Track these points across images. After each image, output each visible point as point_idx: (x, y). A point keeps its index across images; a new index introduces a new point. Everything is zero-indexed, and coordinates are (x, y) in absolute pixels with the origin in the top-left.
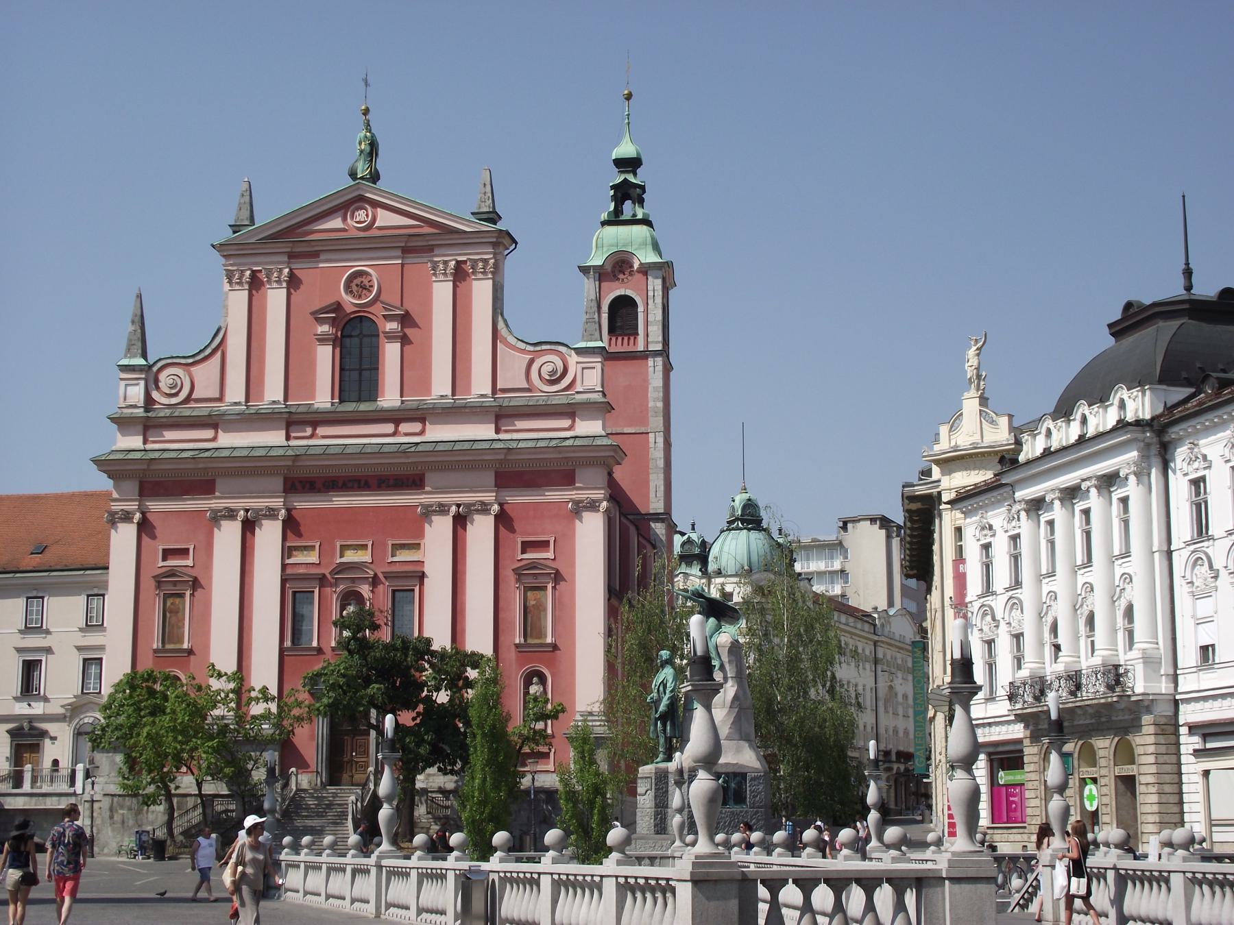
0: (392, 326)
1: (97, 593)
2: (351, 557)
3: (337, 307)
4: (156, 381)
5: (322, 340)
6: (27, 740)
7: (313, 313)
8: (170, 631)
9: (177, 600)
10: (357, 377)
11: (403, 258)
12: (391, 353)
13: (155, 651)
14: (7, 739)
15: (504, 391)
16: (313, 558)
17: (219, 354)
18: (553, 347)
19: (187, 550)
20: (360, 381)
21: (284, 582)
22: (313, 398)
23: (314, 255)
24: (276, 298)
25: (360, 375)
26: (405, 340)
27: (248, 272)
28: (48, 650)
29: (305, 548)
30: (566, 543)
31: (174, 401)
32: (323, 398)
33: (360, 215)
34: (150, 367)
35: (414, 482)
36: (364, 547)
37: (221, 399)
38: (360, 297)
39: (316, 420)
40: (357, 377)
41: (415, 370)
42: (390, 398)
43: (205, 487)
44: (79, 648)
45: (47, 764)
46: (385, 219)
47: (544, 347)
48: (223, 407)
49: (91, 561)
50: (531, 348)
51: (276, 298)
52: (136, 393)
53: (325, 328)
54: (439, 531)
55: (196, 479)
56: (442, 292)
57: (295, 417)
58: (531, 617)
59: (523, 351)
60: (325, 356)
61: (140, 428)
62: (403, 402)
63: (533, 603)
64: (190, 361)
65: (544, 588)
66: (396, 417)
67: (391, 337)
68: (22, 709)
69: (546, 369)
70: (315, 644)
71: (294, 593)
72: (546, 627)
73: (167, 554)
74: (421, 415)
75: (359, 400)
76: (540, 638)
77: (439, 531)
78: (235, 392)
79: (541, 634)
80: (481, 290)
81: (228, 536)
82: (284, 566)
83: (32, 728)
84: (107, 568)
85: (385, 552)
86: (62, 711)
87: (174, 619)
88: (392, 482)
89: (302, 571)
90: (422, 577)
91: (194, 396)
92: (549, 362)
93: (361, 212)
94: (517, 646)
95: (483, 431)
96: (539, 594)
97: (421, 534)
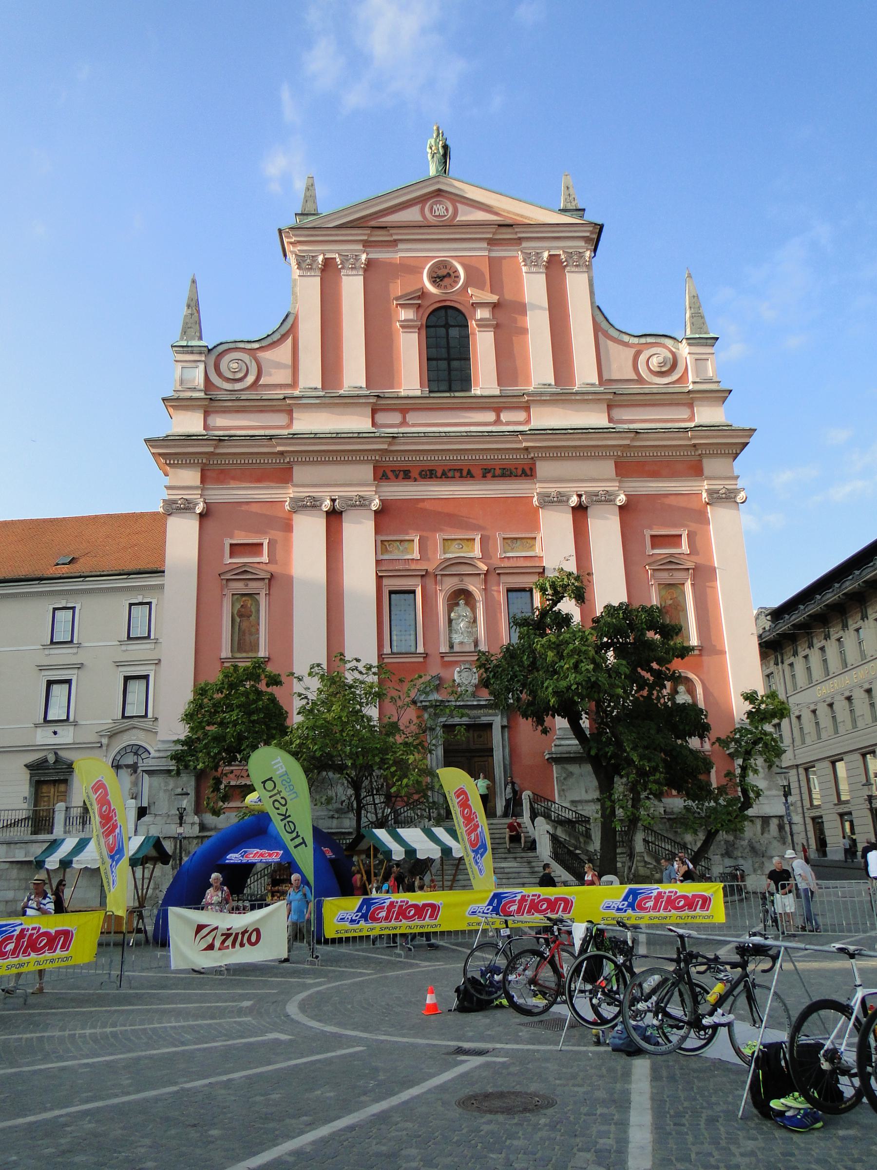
3: (423, 294)
5: (406, 326)
6: (50, 776)
8: (243, 639)
10: (448, 364)
11: (490, 251)
14: (25, 775)
17: (289, 341)
19: (262, 544)
21: (379, 578)
24: (352, 287)
31: (238, 386)
33: (439, 209)
34: (210, 351)
35: (527, 473)
37: (294, 384)
40: (448, 364)
44: (119, 664)
47: (649, 340)
48: (297, 393)
50: (636, 341)
52: (197, 376)
59: (626, 344)
63: (670, 602)
64: (256, 346)
66: (496, 404)
67: (483, 324)
68: (44, 737)
69: (654, 362)
70: (421, 649)
71: (391, 592)
73: (235, 549)
78: (311, 377)
80: (576, 285)
82: (378, 562)
87: (245, 624)
88: (498, 472)
92: (657, 357)
97: (536, 527)
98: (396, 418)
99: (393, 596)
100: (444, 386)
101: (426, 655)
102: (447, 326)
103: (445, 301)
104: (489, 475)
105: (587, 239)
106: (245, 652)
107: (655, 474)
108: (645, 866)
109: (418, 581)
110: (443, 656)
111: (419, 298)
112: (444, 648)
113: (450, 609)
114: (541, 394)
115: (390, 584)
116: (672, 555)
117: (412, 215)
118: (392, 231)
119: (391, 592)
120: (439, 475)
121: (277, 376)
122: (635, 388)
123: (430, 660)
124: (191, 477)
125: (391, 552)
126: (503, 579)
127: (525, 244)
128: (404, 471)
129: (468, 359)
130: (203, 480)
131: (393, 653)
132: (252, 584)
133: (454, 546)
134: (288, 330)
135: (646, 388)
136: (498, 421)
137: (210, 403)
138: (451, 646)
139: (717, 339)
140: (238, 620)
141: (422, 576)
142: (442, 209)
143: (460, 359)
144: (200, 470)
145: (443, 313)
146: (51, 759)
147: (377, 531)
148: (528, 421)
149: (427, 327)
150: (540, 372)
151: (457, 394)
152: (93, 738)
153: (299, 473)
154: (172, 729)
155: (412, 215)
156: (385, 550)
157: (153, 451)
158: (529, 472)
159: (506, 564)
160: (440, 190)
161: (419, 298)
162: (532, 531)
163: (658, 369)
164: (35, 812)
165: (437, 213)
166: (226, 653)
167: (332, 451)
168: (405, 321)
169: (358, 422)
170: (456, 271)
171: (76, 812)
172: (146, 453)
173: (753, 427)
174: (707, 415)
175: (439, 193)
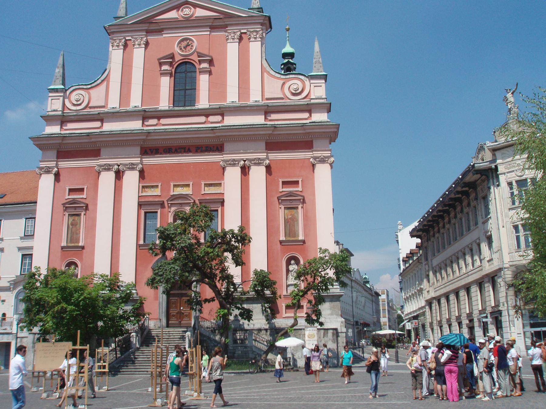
0: (205, 65)
1: (31, 217)
2: (179, 191)
4: (69, 98)
5: (163, 74)
7: (159, 59)
9: (76, 218)
10: (184, 92)
12: (203, 81)
13: (63, 248)
15: (267, 99)
16: (157, 192)
18: (296, 76)
19: (83, 189)
20: (185, 95)
22: (158, 104)
23: (160, 31)
24: (139, 54)
25: (185, 92)
26: (210, 73)
29: (153, 187)
30: (310, 182)
31: (79, 108)
32: (164, 103)
35: (218, 148)
36: (188, 185)
38: (186, 52)
39: (160, 115)
40: (184, 92)
41: (218, 87)
42: (203, 102)
43: (95, 153)
46: (200, 13)
49: (29, 200)
51: (139, 54)
53: (165, 67)
54: (233, 175)
55: (89, 148)
57: (148, 114)
58: (290, 224)
60: (166, 83)
61: (59, 122)
62: (210, 105)
63: (290, 217)
65: (297, 208)
66: (206, 113)
67: (203, 71)
71: (146, 213)
72: (298, 231)
73: (71, 191)
74: (222, 112)
75: (185, 106)
76: (295, 237)
77: (233, 175)
79: (295, 234)
81: (107, 180)
82: (139, 196)
85: (201, 188)
88: (204, 149)
90: (222, 203)
91: (90, 105)
93: (187, 10)
94: (281, 242)
95: (258, 120)
96: (294, 211)
98: (154, 121)
99: (148, 214)
103: (185, 59)
104: (199, 151)
105: (262, 24)
106: (73, 243)
108: (253, 353)
109: (159, 207)
117: (173, 14)
118: (160, 24)
120: (173, 151)
125: (147, 192)
128: (156, 150)
129: (195, 89)
139: (326, 75)
140: (71, 227)
141: (161, 204)
142: (187, 11)
144: (56, 152)
152: (8, 285)
155: (173, 14)
157: (35, 143)
158: (220, 149)
162: (219, 180)
163: (294, 92)
165: (185, 13)
168: (164, 70)
173: (338, 122)
174: (320, 117)
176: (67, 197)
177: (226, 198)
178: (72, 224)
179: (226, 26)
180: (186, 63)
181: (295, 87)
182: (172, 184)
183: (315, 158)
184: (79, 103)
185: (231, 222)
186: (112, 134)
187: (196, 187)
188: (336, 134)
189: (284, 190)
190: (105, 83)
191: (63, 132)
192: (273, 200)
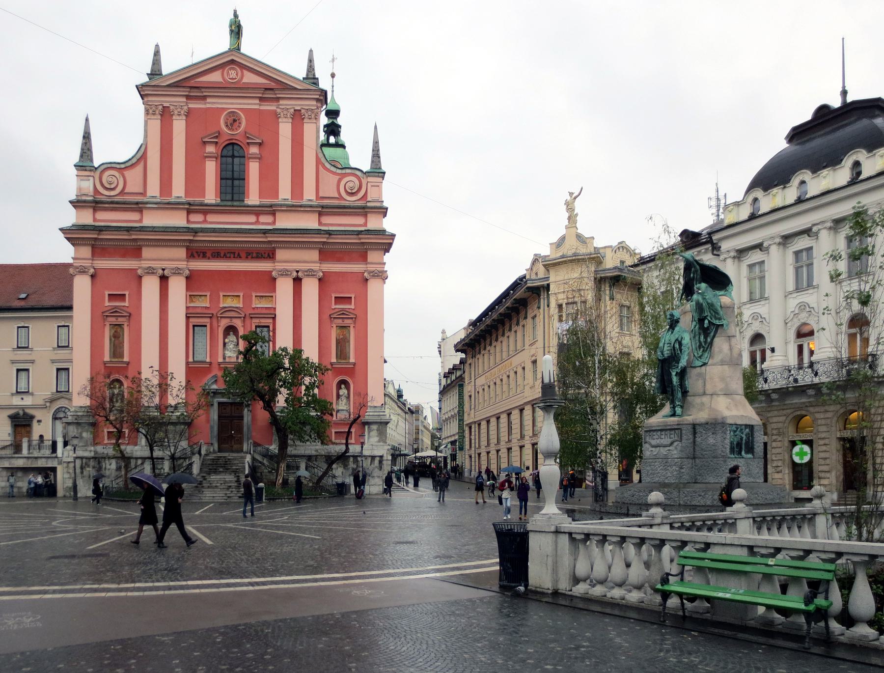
0: (254, 150)
2: (229, 303)
3: (219, 134)
5: (210, 157)
6: (21, 422)
8: (117, 351)
12: (253, 169)
18: (353, 171)
19: (124, 295)
21: (188, 318)
24: (179, 126)
26: (260, 158)
27: (161, 107)
28: (33, 362)
31: (113, 193)
32: (211, 196)
33: (233, 74)
35: (270, 255)
39: (206, 210)
42: (253, 198)
45: (35, 437)
46: (250, 78)
47: (348, 171)
48: (146, 200)
50: (339, 171)
51: (179, 126)
54: (284, 287)
56: (285, 129)
58: (342, 344)
60: (211, 169)
66: (257, 211)
67: (254, 157)
71: (194, 326)
74: (272, 210)
76: (345, 359)
77: (284, 287)
81: (150, 287)
82: (187, 308)
83: (25, 414)
84: (70, 308)
86: (42, 402)
89: (199, 311)
96: (345, 331)
97: (274, 290)
98: (198, 218)
100: (229, 197)
101: (210, 364)
102: (233, 156)
105: (318, 100)
107: (340, 260)
109: (208, 320)
110: (219, 364)
111: (217, 137)
112: (221, 360)
113: (225, 337)
114: (281, 206)
115: (193, 321)
116: (343, 309)
117: (215, 77)
119: (194, 326)
121: (134, 186)
122: (336, 202)
123: (213, 365)
124: (86, 251)
126: (254, 320)
127: (281, 102)
130: (93, 254)
131: (194, 361)
132: (120, 319)
133: (229, 300)
134: (141, 157)
135: (343, 203)
136: (257, 222)
137: (96, 205)
138: (224, 358)
143: (239, 179)
145: (230, 147)
146: (21, 413)
147: (188, 289)
148: (274, 223)
149: (222, 156)
150: (285, 193)
151: (235, 203)
153: (146, 252)
154: (80, 400)
156: (192, 301)
159: (256, 311)
160: (233, 60)
161: (217, 137)
164: (15, 441)
166: (107, 358)
167: (165, 237)
169: (178, 220)
170: (240, 116)
171: (35, 443)
172: (61, 235)
175: (233, 62)
176: (107, 304)
177: (278, 313)
178: (115, 337)
179: (278, 99)
180: (233, 144)
181: (351, 184)
182: (221, 294)
183: (370, 272)
184: (112, 186)
185: (284, 339)
186: (153, 230)
187: (247, 299)
188: (390, 245)
189: (337, 306)
190: (142, 163)
191: (97, 224)
192: (325, 318)
